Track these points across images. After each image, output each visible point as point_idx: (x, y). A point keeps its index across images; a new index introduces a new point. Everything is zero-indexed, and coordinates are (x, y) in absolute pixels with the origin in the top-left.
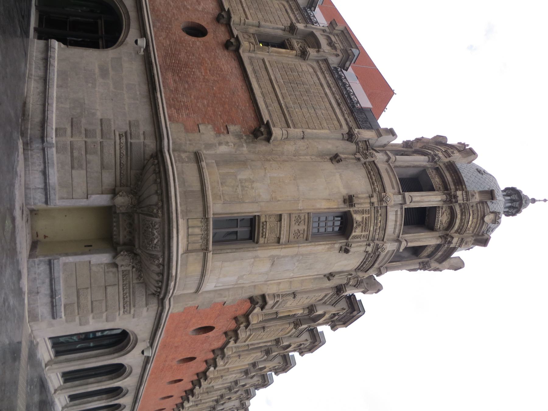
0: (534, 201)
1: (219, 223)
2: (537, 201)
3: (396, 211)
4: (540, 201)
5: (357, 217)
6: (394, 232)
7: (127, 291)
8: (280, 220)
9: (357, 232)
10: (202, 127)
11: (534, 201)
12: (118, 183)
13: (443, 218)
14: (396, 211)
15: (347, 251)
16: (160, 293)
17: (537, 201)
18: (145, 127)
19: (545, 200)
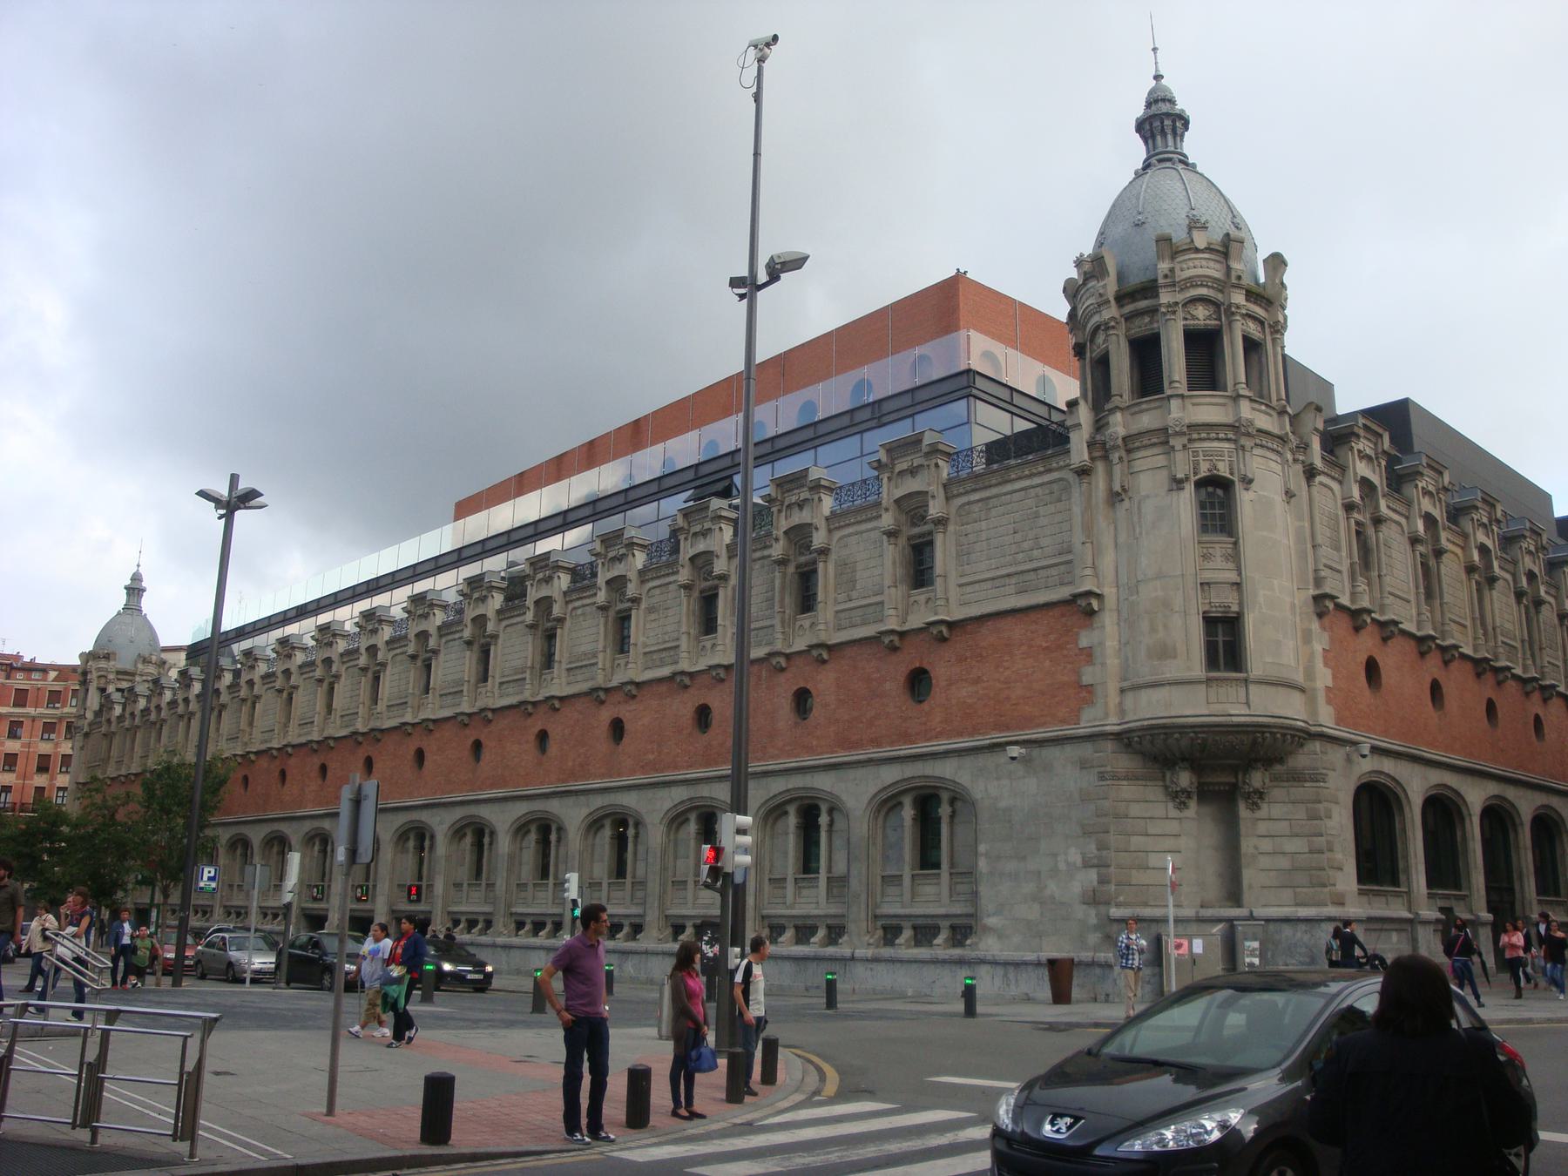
0: (1158, 77)
1: (1212, 661)
4: (1156, 63)
5: (1204, 471)
6: (1224, 405)
8: (1208, 584)
9: (1223, 470)
10: (1086, 680)
11: (1158, 77)
12: (1161, 783)
13: (1201, 315)
14: (1194, 404)
15: (1251, 481)
16: (1300, 738)
18: (1087, 750)
19: (1155, 49)
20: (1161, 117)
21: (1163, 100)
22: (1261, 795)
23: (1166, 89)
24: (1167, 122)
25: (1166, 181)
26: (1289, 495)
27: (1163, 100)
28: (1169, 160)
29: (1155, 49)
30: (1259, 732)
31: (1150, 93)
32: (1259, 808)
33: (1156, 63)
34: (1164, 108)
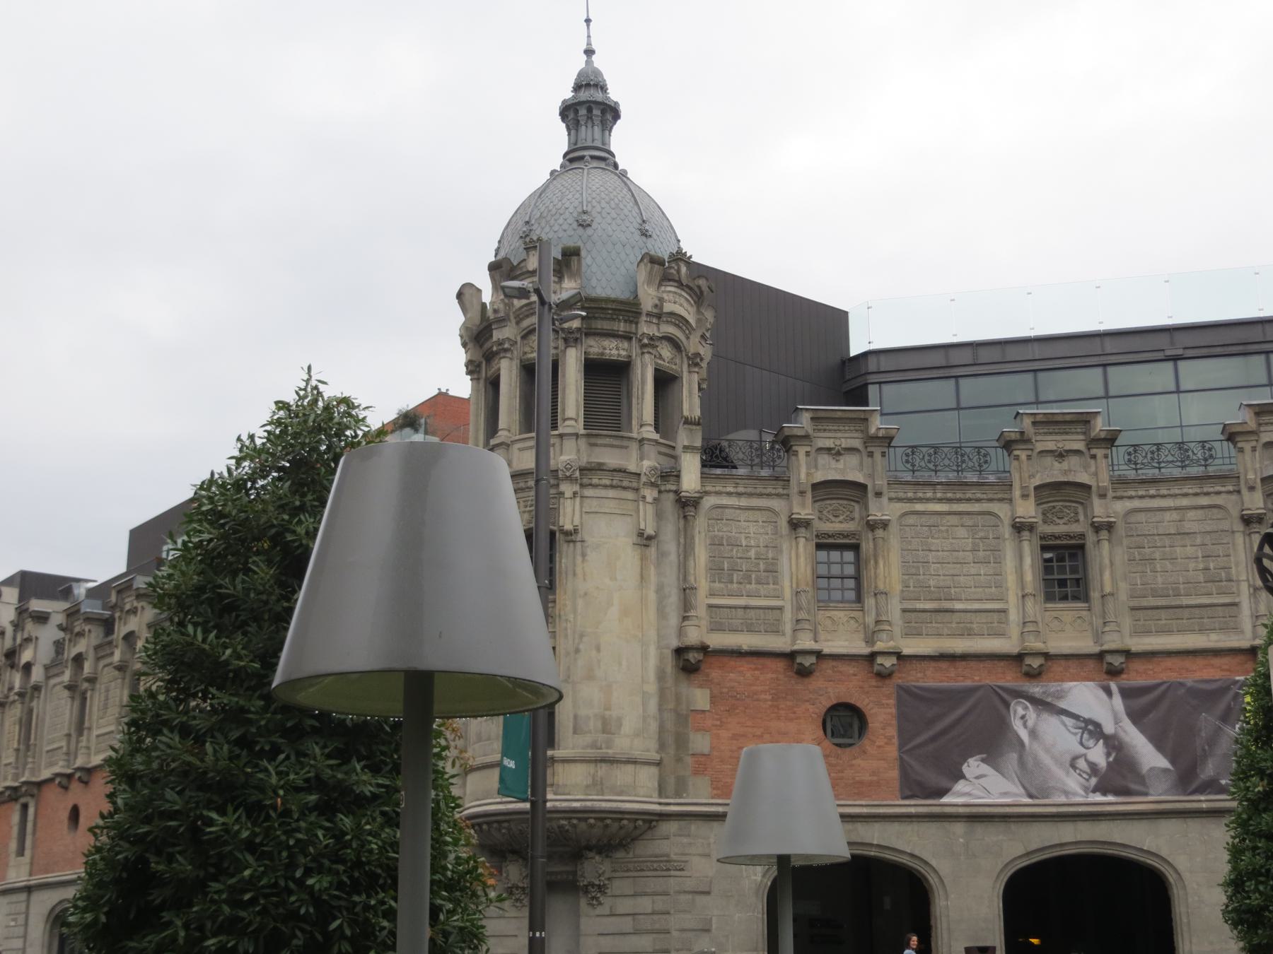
2: (589, 44)
3: (520, 450)
7: (631, 866)
17: (589, 44)
19: (588, 21)
20: (590, 105)
21: (596, 86)
22: (601, 889)
23: (597, 73)
24: (596, 112)
25: (594, 179)
26: (645, 540)
27: (596, 86)
28: (581, 158)
29: (588, 21)
30: (563, 819)
31: (580, 75)
32: (600, 904)
33: (589, 36)
34: (598, 96)
